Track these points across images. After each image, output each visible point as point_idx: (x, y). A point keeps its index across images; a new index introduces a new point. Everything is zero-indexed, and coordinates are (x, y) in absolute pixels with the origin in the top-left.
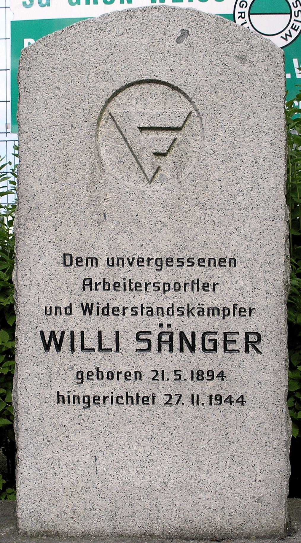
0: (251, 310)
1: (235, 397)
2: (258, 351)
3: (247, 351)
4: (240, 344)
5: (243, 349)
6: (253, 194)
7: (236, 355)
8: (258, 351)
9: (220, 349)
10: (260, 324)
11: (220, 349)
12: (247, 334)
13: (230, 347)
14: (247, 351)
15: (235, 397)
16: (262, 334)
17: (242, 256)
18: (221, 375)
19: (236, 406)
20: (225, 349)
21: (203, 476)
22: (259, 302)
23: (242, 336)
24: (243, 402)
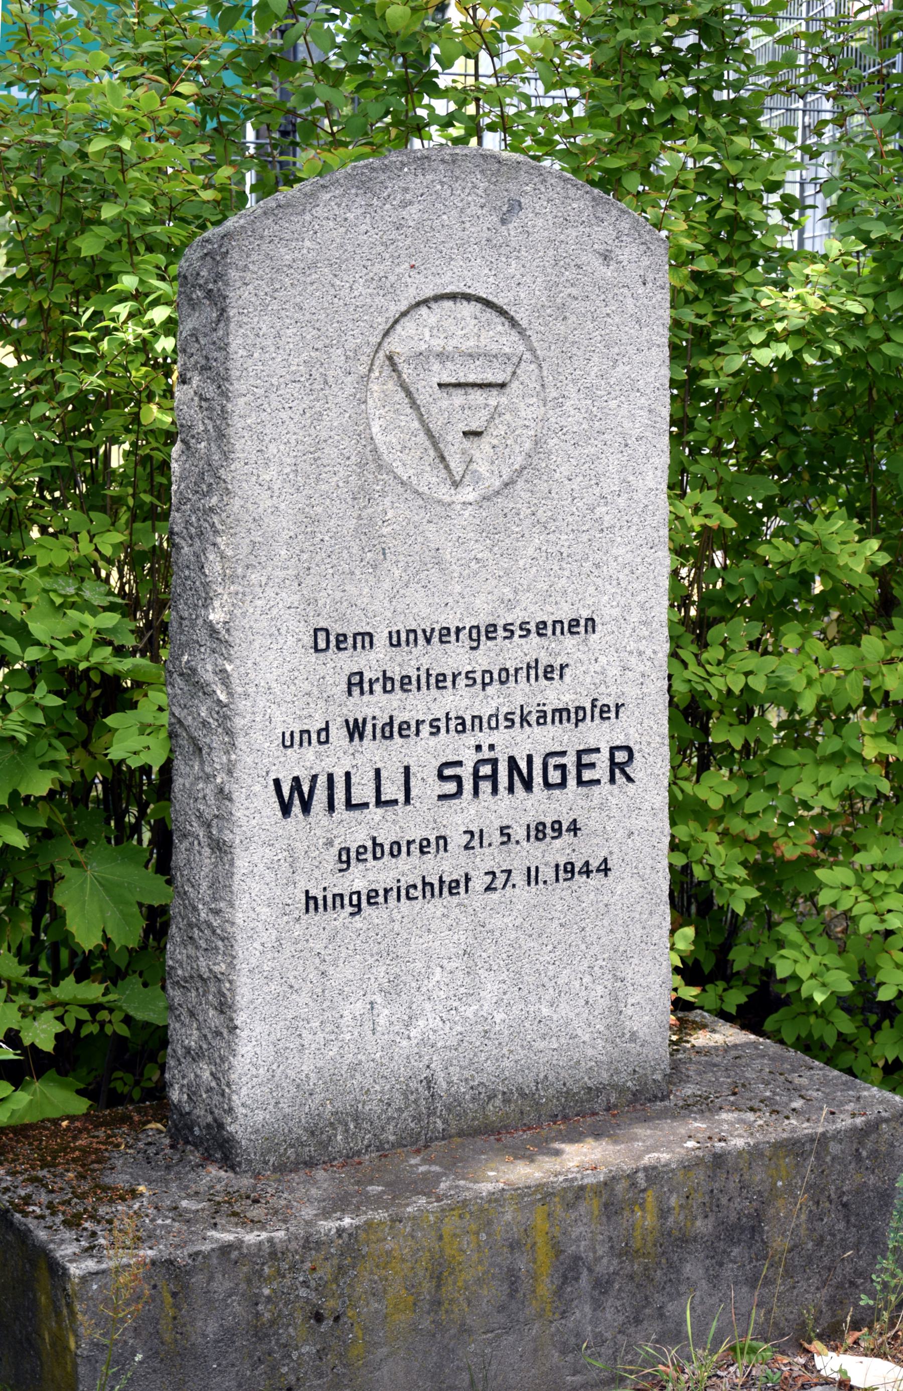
0: (618, 707)
1: (594, 864)
2: (630, 779)
3: (612, 780)
4: (601, 771)
5: (605, 778)
6: (621, 502)
7: (595, 789)
8: (630, 779)
9: (572, 781)
10: (632, 731)
11: (572, 781)
12: (613, 750)
13: (587, 775)
14: (612, 780)
15: (594, 864)
16: (635, 748)
17: (606, 613)
18: (574, 828)
19: (597, 879)
20: (580, 782)
21: (545, 1011)
22: (631, 693)
23: (605, 754)
24: (606, 871)
